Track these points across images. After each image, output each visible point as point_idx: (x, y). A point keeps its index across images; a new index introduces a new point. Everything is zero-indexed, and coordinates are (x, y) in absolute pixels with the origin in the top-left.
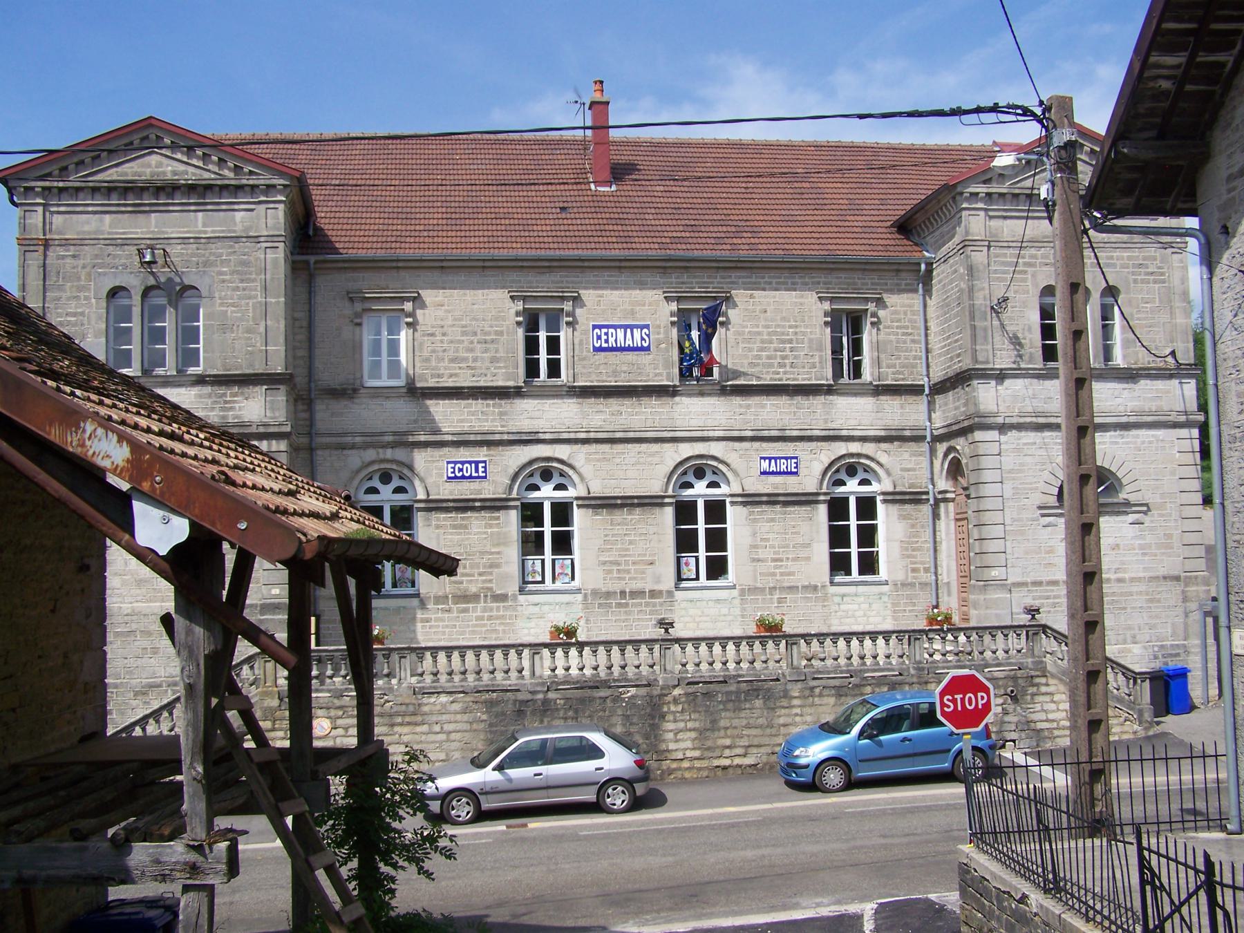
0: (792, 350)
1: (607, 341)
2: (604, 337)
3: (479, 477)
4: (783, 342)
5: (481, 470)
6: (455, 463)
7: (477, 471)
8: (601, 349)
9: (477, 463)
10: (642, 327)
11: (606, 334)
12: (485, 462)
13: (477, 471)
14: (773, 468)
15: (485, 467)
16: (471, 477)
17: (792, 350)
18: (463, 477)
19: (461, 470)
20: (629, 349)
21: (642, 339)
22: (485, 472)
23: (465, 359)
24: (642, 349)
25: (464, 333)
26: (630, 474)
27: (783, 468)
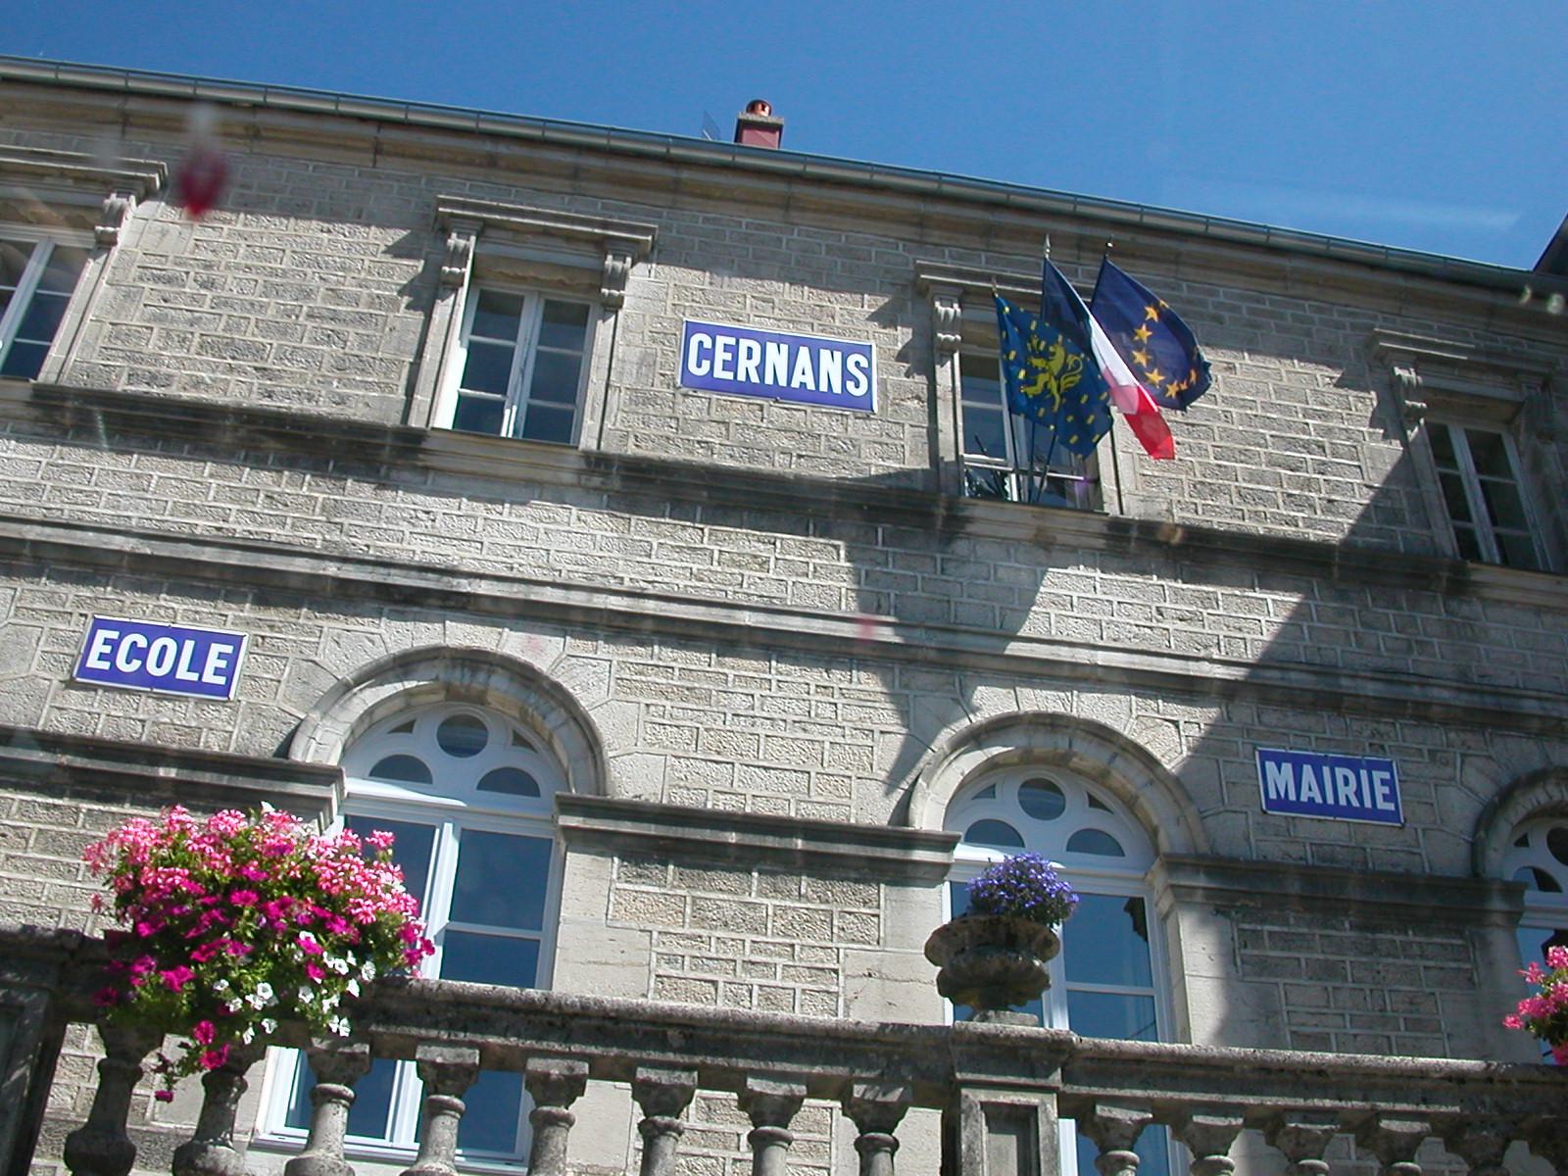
0: (1322, 468)
1: (731, 366)
2: (721, 356)
3: (199, 686)
4: (1292, 444)
5: (213, 661)
6: (125, 628)
7: (198, 663)
8: (710, 384)
9: (204, 641)
10: (847, 351)
11: (733, 350)
12: (236, 641)
13: (198, 663)
14: (1310, 791)
15: (232, 660)
16: (170, 681)
17: (1322, 468)
18: (142, 677)
19: (137, 652)
20: (802, 395)
21: (846, 375)
22: (228, 673)
23: (258, 351)
24: (845, 401)
25: (270, 289)
26: (773, 753)
27: (1346, 793)
